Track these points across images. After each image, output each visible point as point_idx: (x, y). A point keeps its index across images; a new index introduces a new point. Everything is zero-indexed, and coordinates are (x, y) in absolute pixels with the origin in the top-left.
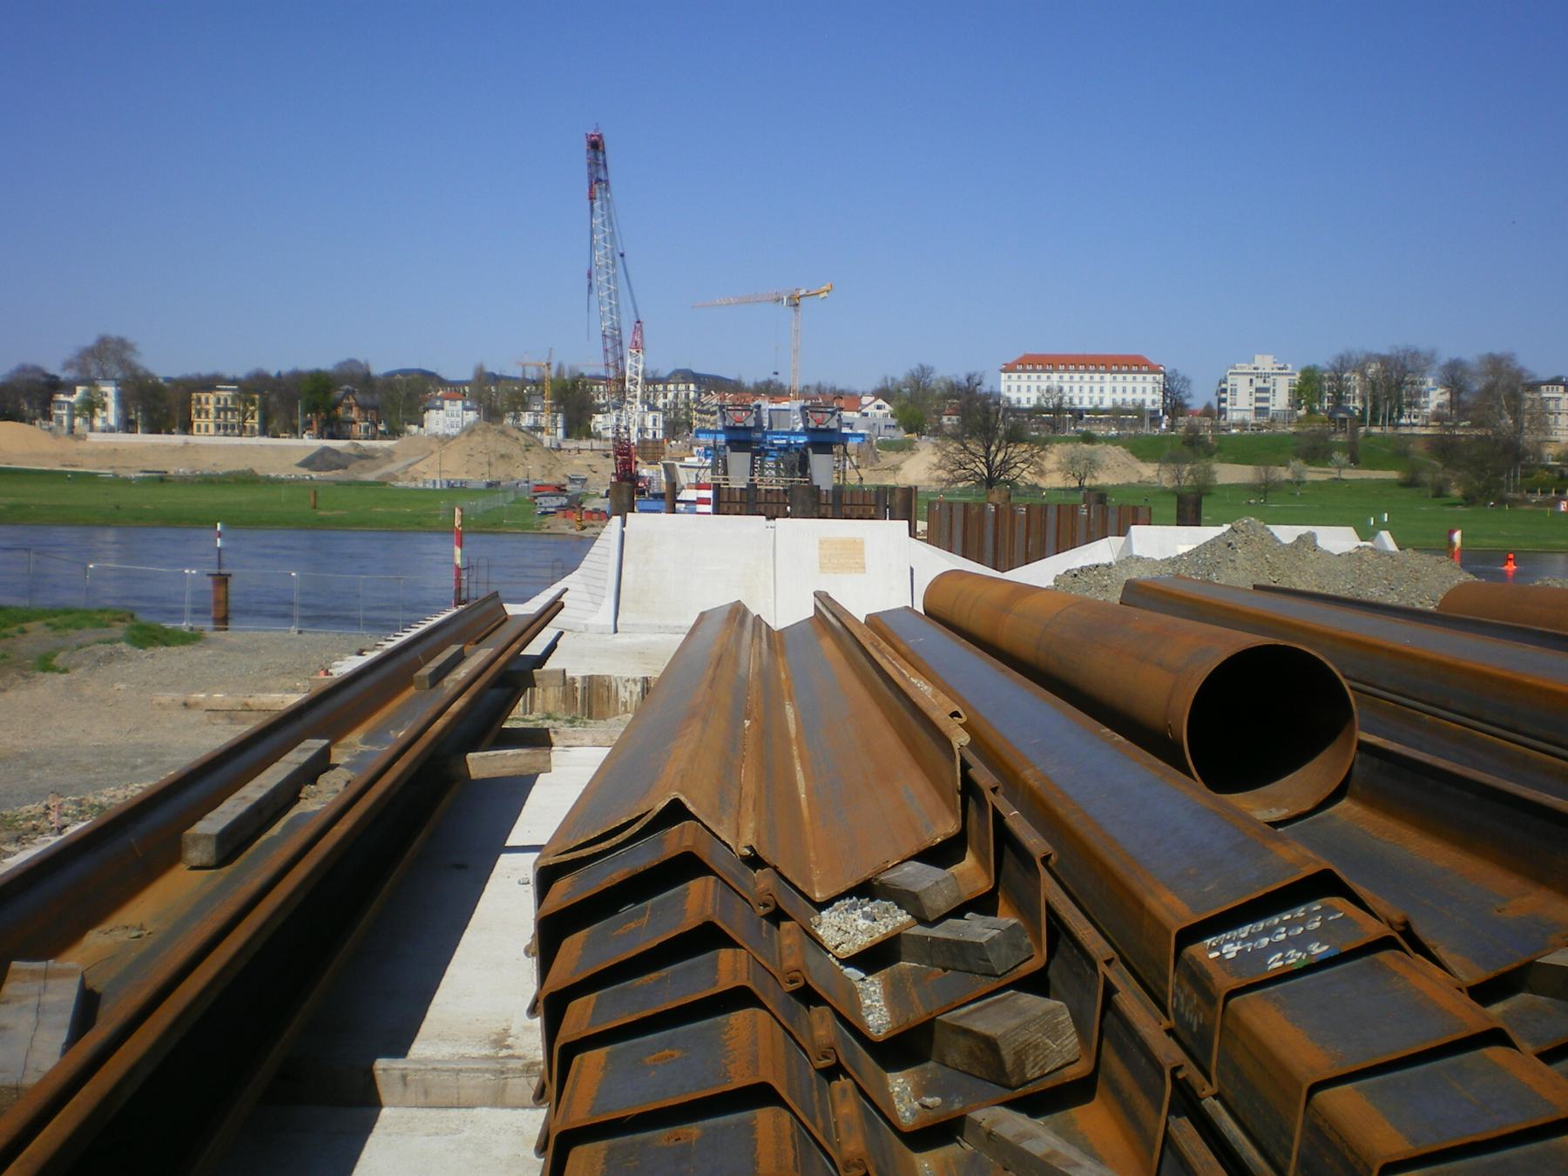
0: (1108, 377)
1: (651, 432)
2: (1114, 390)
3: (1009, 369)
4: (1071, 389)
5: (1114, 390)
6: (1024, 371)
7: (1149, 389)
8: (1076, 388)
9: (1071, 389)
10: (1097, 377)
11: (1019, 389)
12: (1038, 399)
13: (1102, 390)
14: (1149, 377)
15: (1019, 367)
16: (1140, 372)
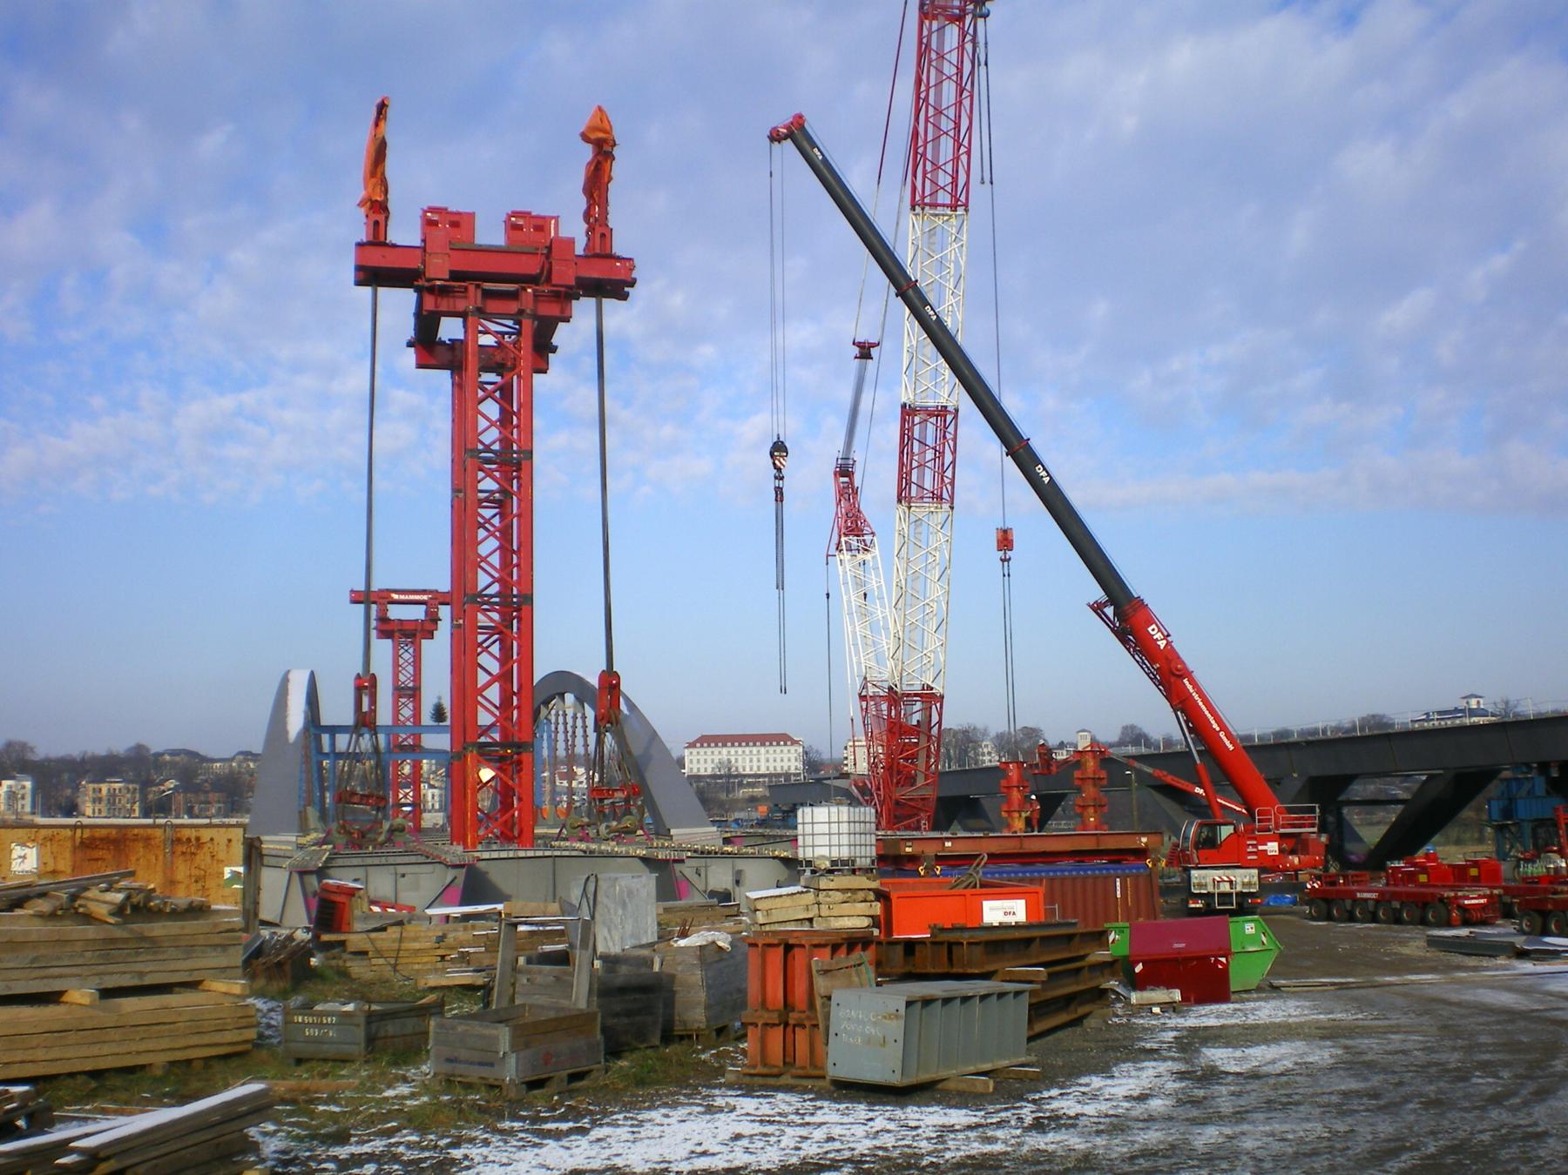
0: (763, 750)
1: (430, 804)
2: (768, 761)
3: (692, 745)
4: (736, 760)
5: (768, 761)
6: (702, 746)
7: (793, 760)
8: (740, 758)
9: (736, 760)
10: (755, 750)
11: (698, 761)
12: (713, 768)
13: (759, 761)
14: (792, 749)
15: (698, 745)
16: (785, 744)
